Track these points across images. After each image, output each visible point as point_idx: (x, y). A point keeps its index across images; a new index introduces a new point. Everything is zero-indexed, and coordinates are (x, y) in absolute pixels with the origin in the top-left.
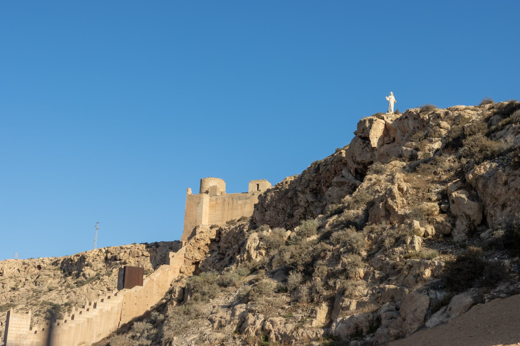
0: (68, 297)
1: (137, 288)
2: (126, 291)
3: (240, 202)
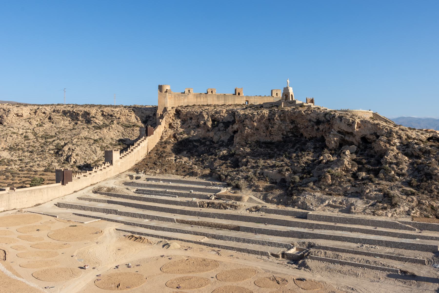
0: (97, 135)
1: (152, 136)
2: (148, 138)
3: (182, 97)
